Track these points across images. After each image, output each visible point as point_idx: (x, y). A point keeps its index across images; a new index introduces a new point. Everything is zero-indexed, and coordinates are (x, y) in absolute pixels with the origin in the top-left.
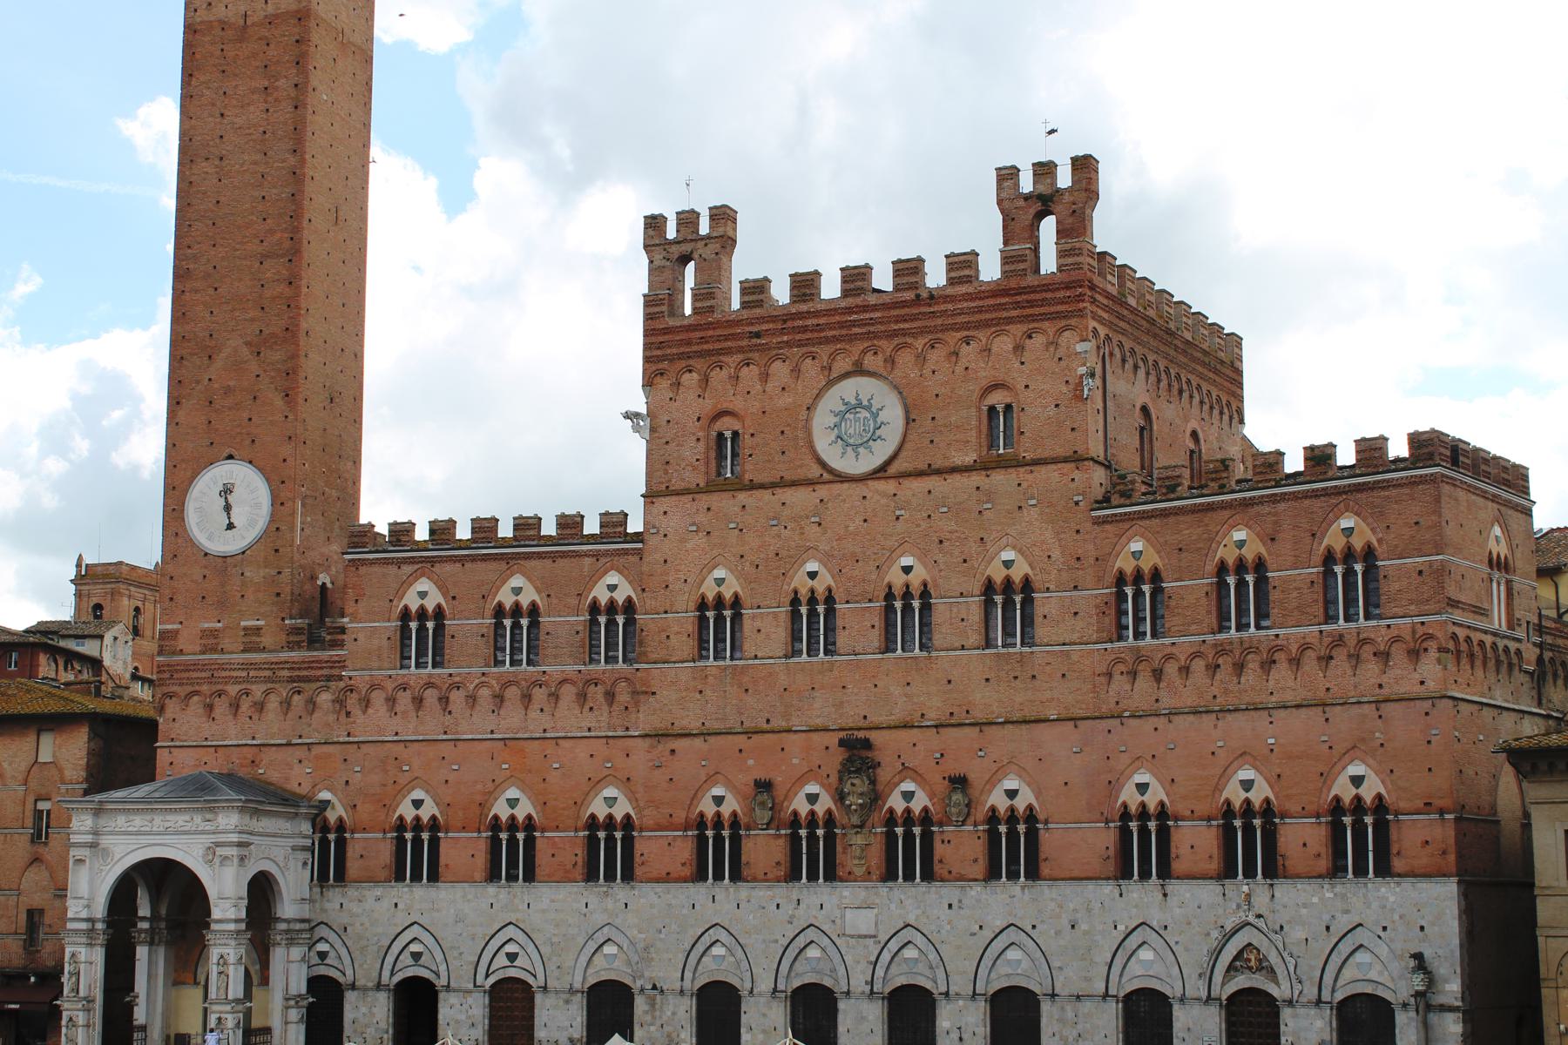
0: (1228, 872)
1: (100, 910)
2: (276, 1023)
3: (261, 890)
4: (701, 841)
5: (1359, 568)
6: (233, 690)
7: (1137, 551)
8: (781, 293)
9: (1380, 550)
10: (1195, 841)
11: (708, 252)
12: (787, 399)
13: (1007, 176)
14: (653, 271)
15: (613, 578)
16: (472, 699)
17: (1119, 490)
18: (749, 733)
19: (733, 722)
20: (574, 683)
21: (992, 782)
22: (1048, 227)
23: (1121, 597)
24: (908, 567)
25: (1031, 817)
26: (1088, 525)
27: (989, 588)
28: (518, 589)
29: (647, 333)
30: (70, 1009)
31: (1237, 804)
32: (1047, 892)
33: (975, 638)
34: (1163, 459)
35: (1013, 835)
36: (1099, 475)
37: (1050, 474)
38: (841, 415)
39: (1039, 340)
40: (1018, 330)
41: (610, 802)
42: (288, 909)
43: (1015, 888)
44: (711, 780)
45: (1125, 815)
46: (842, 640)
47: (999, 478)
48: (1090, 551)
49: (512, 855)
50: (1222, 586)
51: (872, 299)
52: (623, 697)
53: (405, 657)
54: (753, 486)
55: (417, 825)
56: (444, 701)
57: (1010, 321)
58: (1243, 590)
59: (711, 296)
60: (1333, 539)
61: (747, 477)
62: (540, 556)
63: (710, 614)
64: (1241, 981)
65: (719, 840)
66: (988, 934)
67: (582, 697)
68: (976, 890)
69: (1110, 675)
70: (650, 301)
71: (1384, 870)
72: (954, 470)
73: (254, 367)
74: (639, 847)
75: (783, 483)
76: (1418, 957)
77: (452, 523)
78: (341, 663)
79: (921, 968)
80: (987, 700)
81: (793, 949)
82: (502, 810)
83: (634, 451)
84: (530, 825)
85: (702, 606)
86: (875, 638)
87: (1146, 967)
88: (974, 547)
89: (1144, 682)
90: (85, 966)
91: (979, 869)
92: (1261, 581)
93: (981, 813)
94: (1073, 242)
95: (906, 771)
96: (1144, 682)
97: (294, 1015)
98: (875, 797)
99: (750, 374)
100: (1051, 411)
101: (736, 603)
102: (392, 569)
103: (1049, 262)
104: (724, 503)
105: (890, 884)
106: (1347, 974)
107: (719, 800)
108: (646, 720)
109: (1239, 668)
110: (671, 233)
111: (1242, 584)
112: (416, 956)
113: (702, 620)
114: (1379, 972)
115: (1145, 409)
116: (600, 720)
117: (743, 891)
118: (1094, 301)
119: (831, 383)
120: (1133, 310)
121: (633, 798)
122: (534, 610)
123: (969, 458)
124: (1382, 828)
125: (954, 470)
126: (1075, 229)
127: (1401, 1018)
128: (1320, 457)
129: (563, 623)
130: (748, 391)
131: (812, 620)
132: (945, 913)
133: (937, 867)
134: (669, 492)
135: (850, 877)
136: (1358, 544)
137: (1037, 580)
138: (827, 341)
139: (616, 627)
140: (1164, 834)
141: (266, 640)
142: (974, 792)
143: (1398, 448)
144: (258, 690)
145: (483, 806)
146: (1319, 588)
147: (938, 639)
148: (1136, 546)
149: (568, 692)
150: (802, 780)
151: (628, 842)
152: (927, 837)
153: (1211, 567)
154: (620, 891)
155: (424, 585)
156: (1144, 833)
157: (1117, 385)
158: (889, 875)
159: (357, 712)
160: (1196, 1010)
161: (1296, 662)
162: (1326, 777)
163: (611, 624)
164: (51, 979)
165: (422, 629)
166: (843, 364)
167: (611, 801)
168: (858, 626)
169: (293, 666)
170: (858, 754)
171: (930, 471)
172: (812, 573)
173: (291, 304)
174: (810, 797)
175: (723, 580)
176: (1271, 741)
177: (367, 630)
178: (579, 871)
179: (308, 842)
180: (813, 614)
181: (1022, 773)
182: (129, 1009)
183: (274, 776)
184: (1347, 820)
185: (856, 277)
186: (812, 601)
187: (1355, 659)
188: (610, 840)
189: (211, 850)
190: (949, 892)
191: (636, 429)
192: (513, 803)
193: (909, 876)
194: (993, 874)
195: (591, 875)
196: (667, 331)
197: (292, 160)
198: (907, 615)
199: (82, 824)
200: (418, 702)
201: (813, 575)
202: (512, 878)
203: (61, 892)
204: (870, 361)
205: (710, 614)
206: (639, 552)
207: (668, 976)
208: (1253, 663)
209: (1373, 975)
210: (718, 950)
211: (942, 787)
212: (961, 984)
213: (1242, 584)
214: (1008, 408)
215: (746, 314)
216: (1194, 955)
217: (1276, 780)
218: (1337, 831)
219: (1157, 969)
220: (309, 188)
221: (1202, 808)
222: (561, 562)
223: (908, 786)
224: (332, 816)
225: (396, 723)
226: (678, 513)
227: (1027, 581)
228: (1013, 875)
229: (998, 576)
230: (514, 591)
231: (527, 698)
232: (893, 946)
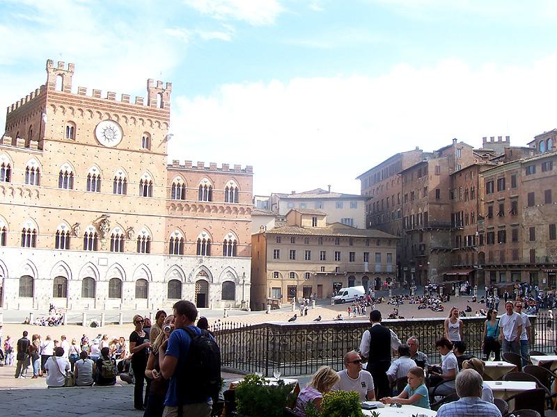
7: (178, 179)
10: (190, 248)
12: (89, 122)
20: (21, 189)
24: (118, 173)
27: (141, 182)
46: (102, 188)
47: (146, 154)
48: (166, 178)
57: (152, 117)
58: (207, 194)
61: (77, 140)
63: (63, 176)
87: (173, 276)
104: (71, 147)
113: (61, 177)
116: (28, 201)
131: (94, 183)
133: (125, 250)
152: (122, 241)
174: (90, 229)
178: (20, 243)
186: (94, 177)
193: (117, 250)
205: (63, 176)
215: (79, 96)
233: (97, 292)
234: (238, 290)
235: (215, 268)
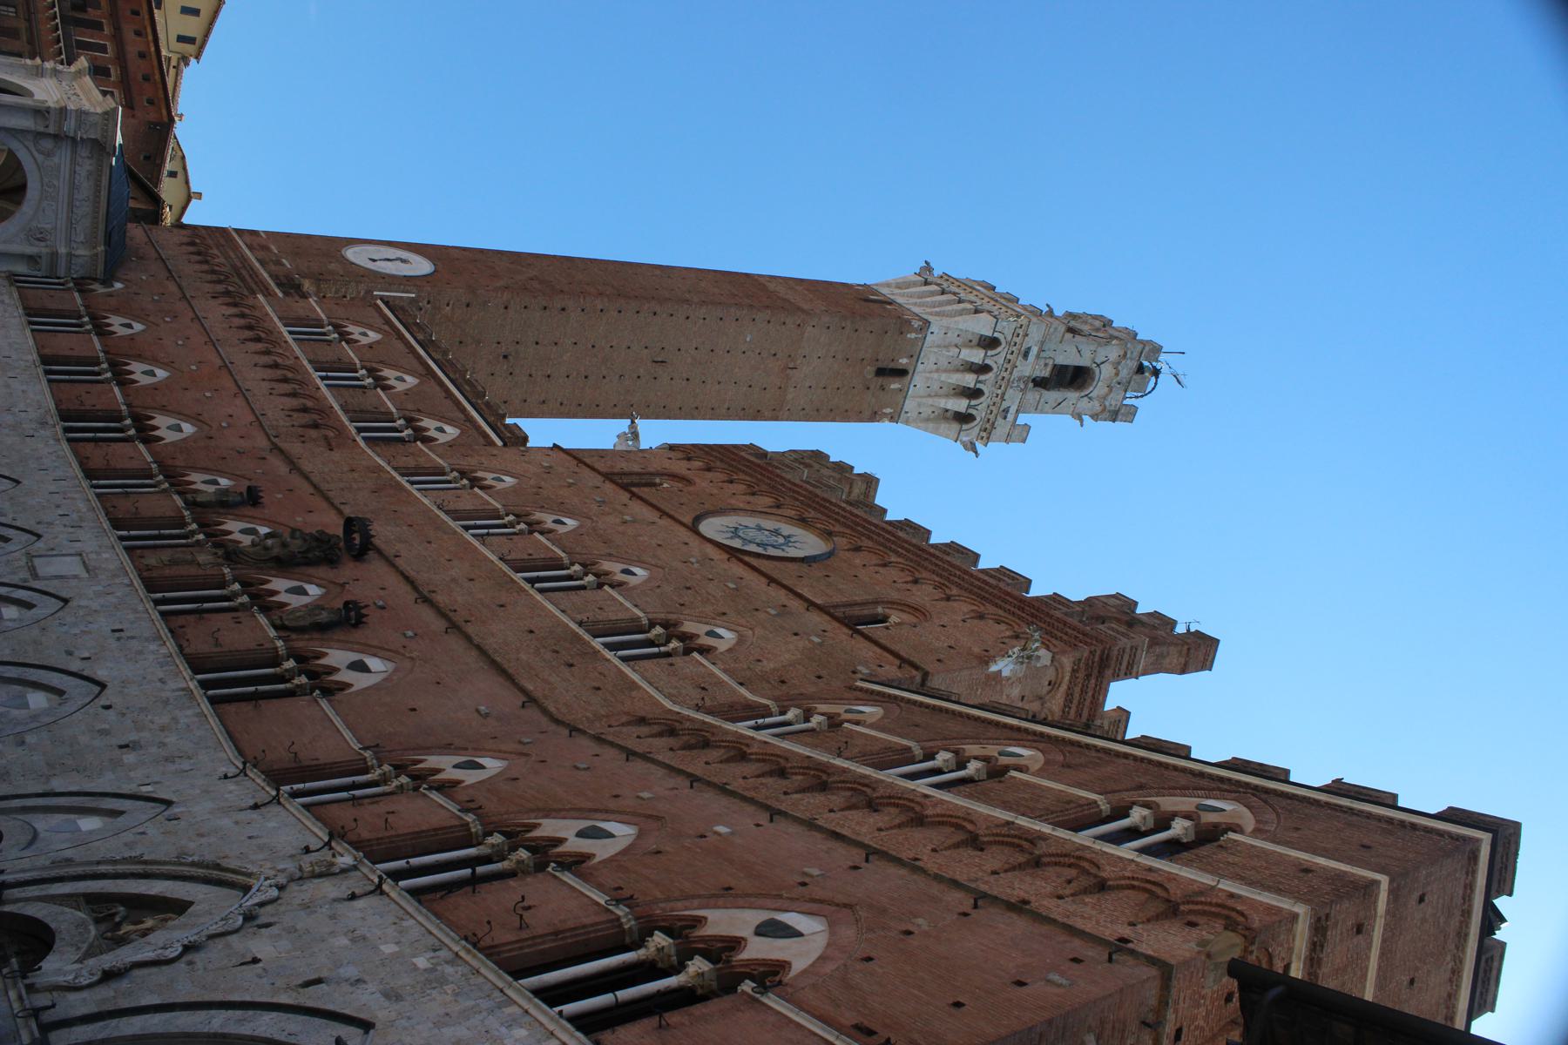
38: (759, 528)
41: (170, 429)
47: (816, 619)
52: (313, 433)
62: (447, 390)
66: (75, 666)
69: (642, 721)
78: (268, 293)
93: (301, 643)
102: (379, 322)
105: (137, 582)
108: (294, 448)
132: (104, 624)
142: (339, 634)
169: (254, 274)
176: (722, 829)
179: (62, 272)
206: (492, 443)
222: (448, 403)
228: (205, 685)
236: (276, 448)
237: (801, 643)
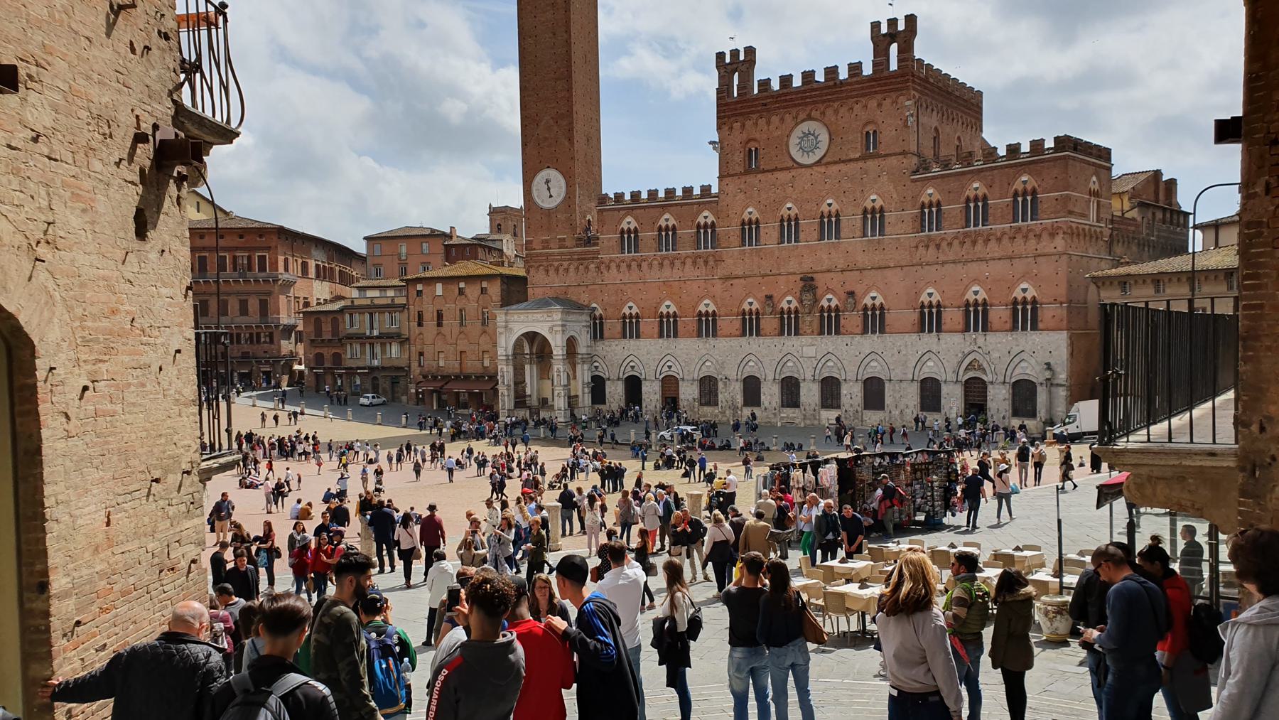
0: (967, 329)
1: (510, 353)
2: (580, 393)
3: (571, 343)
4: (744, 320)
5: (1029, 198)
6: (556, 264)
7: (930, 193)
8: (776, 85)
9: (1039, 190)
10: (953, 316)
11: (743, 68)
13: (876, 26)
14: (720, 78)
15: (706, 213)
16: (651, 265)
17: (924, 166)
18: (763, 276)
19: (756, 272)
21: (865, 294)
22: (894, 48)
23: (923, 213)
24: (830, 204)
25: (882, 307)
26: (909, 183)
27: (865, 211)
28: (667, 219)
29: (718, 106)
30: (502, 389)
31: (971, 301)
32: (888, 339)
33: (859, 233)
34: (943, 152)
35: (874, 315)
36: (915, 160)
37: (893, 161)
38: (802, 138)
39: (888, 101)
40: (879, 96)
41: (707, 306)
42: (582, 349)
43: (875, 337)
44: (747, 296)
45: (923, 306)
46: (802, 236)
47: (871, 164)
49: (668, 327)
50: (968, 208)
51: (815, 86)
52: (711, 263)
53: (623, 249)
54: (764, 171)
55: (631, 316)
56: (639, 266)
57: (876, 92)
58: (977, 210)
59: (745, 88)
60: (1018, 186)
64: (971, 374)
65: (751, 319)
67: (694, 263)
68: (858, 337)
70: (719, 91)
71: (1034, 328)
72: (850, 160)
73: (555, 128)
74: (719, 323)
75: (776, 169)
76: (1048, 364)
77: (639, 192)
78: (598, 252)
79: (835, 369)
80: (863, 259)
81: (782, 363)
82: (663, 310)
83: (715, 156)
84: (675, 315)
85: (743, 224)
86: (816, 235)
87: (931, 369)
88: (858, 194)
89: (932, 250)
90: (506, 373)
91: (859, 330)
92: (985, 205)
93: (860, 307)
94: (906, 55)
95: (829, 290)
96: (932, 250)
97: (586, 390)
98: (816, 301)
99: (762, 122)
100: (894, 132)
101: (757, 222)
103: (894, 66)
106: (1017, 371)
107: (751, 304)
108: (720, 272)
109: (974, 243)
110: (728, 60)
111: (976, 207)
112: (633, 367)
113: (743, 229)
114: (1030, 370)
115: (936, 129)
117: (761, 339)
118: (913, 82)
119: (797, 124)
120: (932, 84)
121: (716, 304)
122: (674, 228)
123: (857, 156)
124: (1034, 310)
125: (850, 160)
126: (906, 49)
127: (1039, 389)
128: (1013, 149)
129: (686, 233)
130: (760, 129)
131: (789, 229)
134: (729, 175)
135: (805, 334)
136: (1029, 188)
137: (886, 208)
138: (795, 106)
139: (708, 234)
140: (939, 314)
141: (567, 243)
143: (1049, 144)
144: (565, 264)
145: (657, 308)
146: (1010, 207)
147: (842, 235)
148: (930, 191)
149: (689, 261)
150: (785, 295)
151: (714, 321)
152: (837, 317)
153: (963, 199)
154: (711, 340)
155: (629, 219)
156: (931, 313)
157: (923, 119)
158: (821, 333)
159: (605, 272)
160: (951, 386)
161: (999, 240)
162: (1011, 289)
163: (706, 232)
164: (493, 378)
165: (629, 237)
166: (802, 116)
167: (707, 305)
168: (809, 228)
170: (808, 284)
171: (841, 161)
172: (790, 208)
173: (569, 100)
174: (788, 302)
175: (752, 212)
177: (608, 239)
180: (789, 225)
181: (878, 290)
182: (524, 388)
183: (574, 298)
184: (1020, 307)
185: (808, 76)
186: (789, 220)
187: (1026, 237)
188: (707, 320)
189: (551, 328)
190: (847, 339)
191: (714, 148)
192: (668, 307)
193: (829, 333)
194: (865, 331)
195: (699, 335)
196: (727, 104)
197: (566, 36)
198: (830, 225)
199: (501, 317)
200: (629, 267)
201: (789, 209)
202: (668, 336)
203: (495, 345)
204: (814, 113)
206: (717, 202)
207: (732, 374)
208: (980, 241)
209: (1028, 371)
210: (751, 364)
211: (844, 296)
212: (851, 376)
213: (976, 207)
214: (875, 132)
216: (951, 363)
217: (989, 291)
218: (1015, 311)
219: (935, 369)
220: (574, 48)
221: (955, 303)
223: (829, 296)
224: (597, 314)
225: (620, 276)
226: (733, 185)
227: (882, 207)
228: (874, 332)
229: (869, 205)
230: (667, 220)
231: (672, 264)
232: (823, 361)
233: (803, 399)
234: (1042, 397)
235: (997, 355)
236: (725, 279)
237: (884, 178)
